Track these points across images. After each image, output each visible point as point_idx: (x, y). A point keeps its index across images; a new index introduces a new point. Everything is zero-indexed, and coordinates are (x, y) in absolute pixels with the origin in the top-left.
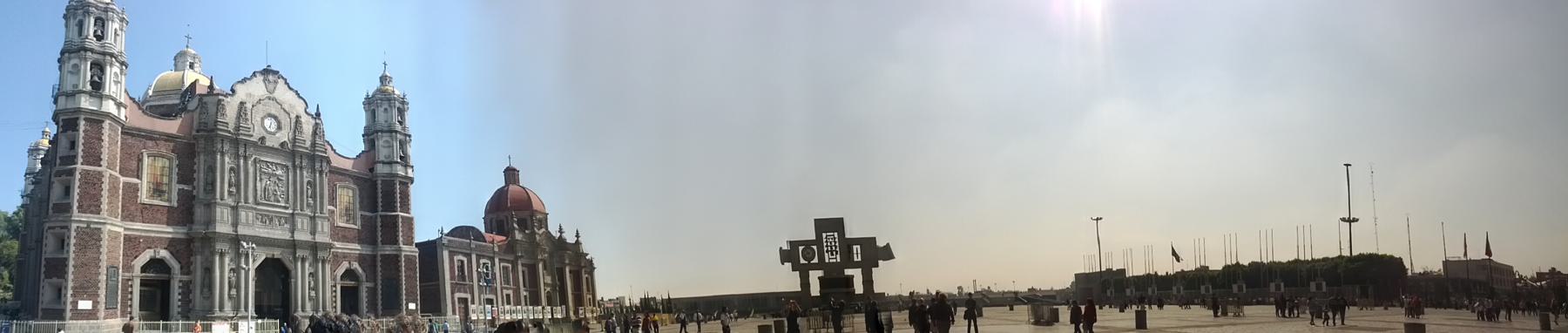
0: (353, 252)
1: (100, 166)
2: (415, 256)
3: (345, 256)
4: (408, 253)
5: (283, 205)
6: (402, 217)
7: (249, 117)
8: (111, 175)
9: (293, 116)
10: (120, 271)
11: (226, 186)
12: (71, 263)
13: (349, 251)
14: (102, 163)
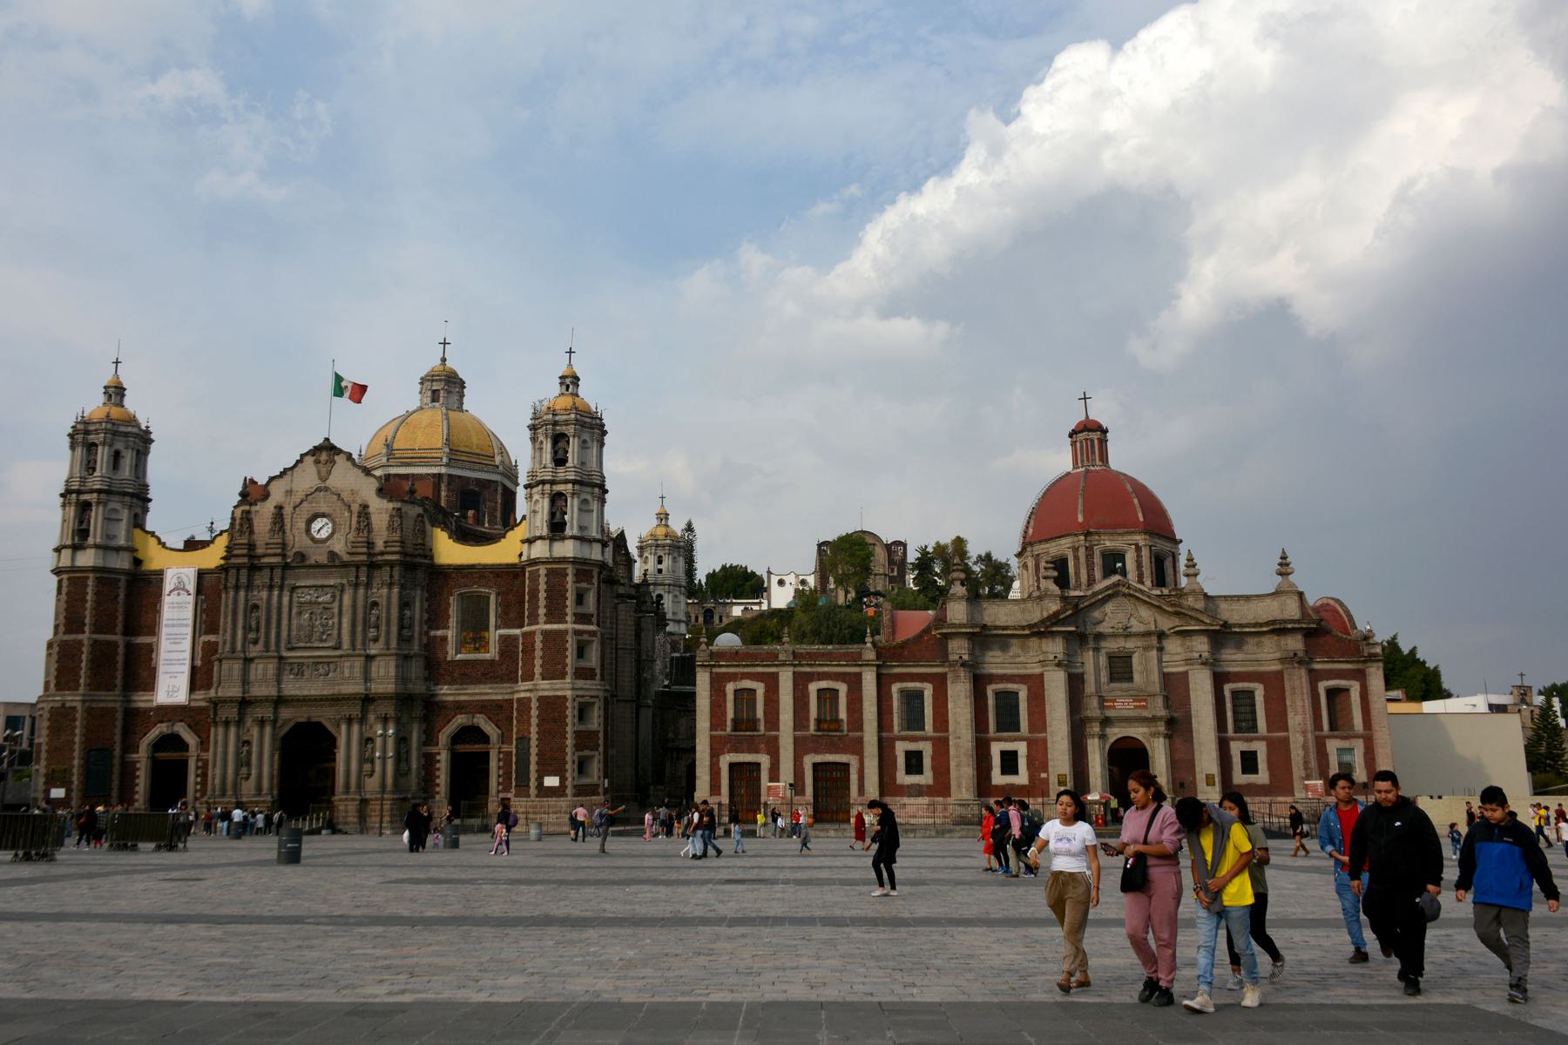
0: (478, 698)
1: (84, 632)
2: (565, 698)
3: (460, 707)
4: (546, 694)
5: (329, 644)
6: (545, 633)
7: (288, 527)
8: (96, 641)
9: (355, 508)
10: (117, 752)
11: (240, 633)
12: (44, 748)
13: (471, 698)
14: (87, 629)
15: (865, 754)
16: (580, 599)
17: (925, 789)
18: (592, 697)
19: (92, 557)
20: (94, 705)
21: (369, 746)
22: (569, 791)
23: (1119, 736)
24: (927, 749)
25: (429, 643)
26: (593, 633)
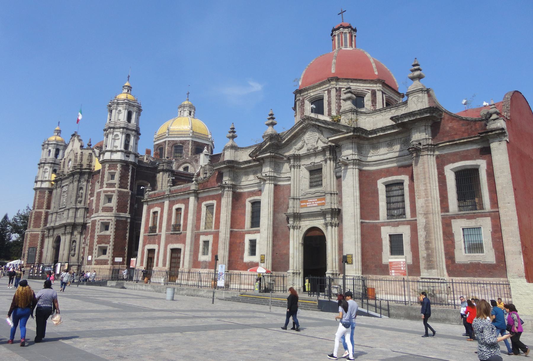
8: (36, 212)
10: (38, 249)
15: (186, 243)
16: (112, 176)
17: (208, 264)
18: (108, 220)
19: (48, 184)
20: (33, 233)
21: (74, 244)
22: (93, 262)
23: (309, 227)
24: (210, 238)
25: (90, 203)
26: (114, 192)
